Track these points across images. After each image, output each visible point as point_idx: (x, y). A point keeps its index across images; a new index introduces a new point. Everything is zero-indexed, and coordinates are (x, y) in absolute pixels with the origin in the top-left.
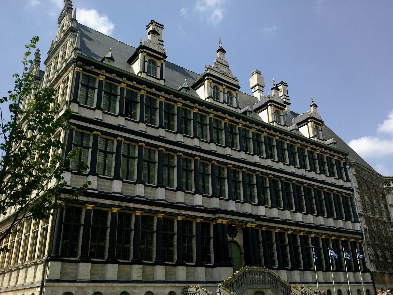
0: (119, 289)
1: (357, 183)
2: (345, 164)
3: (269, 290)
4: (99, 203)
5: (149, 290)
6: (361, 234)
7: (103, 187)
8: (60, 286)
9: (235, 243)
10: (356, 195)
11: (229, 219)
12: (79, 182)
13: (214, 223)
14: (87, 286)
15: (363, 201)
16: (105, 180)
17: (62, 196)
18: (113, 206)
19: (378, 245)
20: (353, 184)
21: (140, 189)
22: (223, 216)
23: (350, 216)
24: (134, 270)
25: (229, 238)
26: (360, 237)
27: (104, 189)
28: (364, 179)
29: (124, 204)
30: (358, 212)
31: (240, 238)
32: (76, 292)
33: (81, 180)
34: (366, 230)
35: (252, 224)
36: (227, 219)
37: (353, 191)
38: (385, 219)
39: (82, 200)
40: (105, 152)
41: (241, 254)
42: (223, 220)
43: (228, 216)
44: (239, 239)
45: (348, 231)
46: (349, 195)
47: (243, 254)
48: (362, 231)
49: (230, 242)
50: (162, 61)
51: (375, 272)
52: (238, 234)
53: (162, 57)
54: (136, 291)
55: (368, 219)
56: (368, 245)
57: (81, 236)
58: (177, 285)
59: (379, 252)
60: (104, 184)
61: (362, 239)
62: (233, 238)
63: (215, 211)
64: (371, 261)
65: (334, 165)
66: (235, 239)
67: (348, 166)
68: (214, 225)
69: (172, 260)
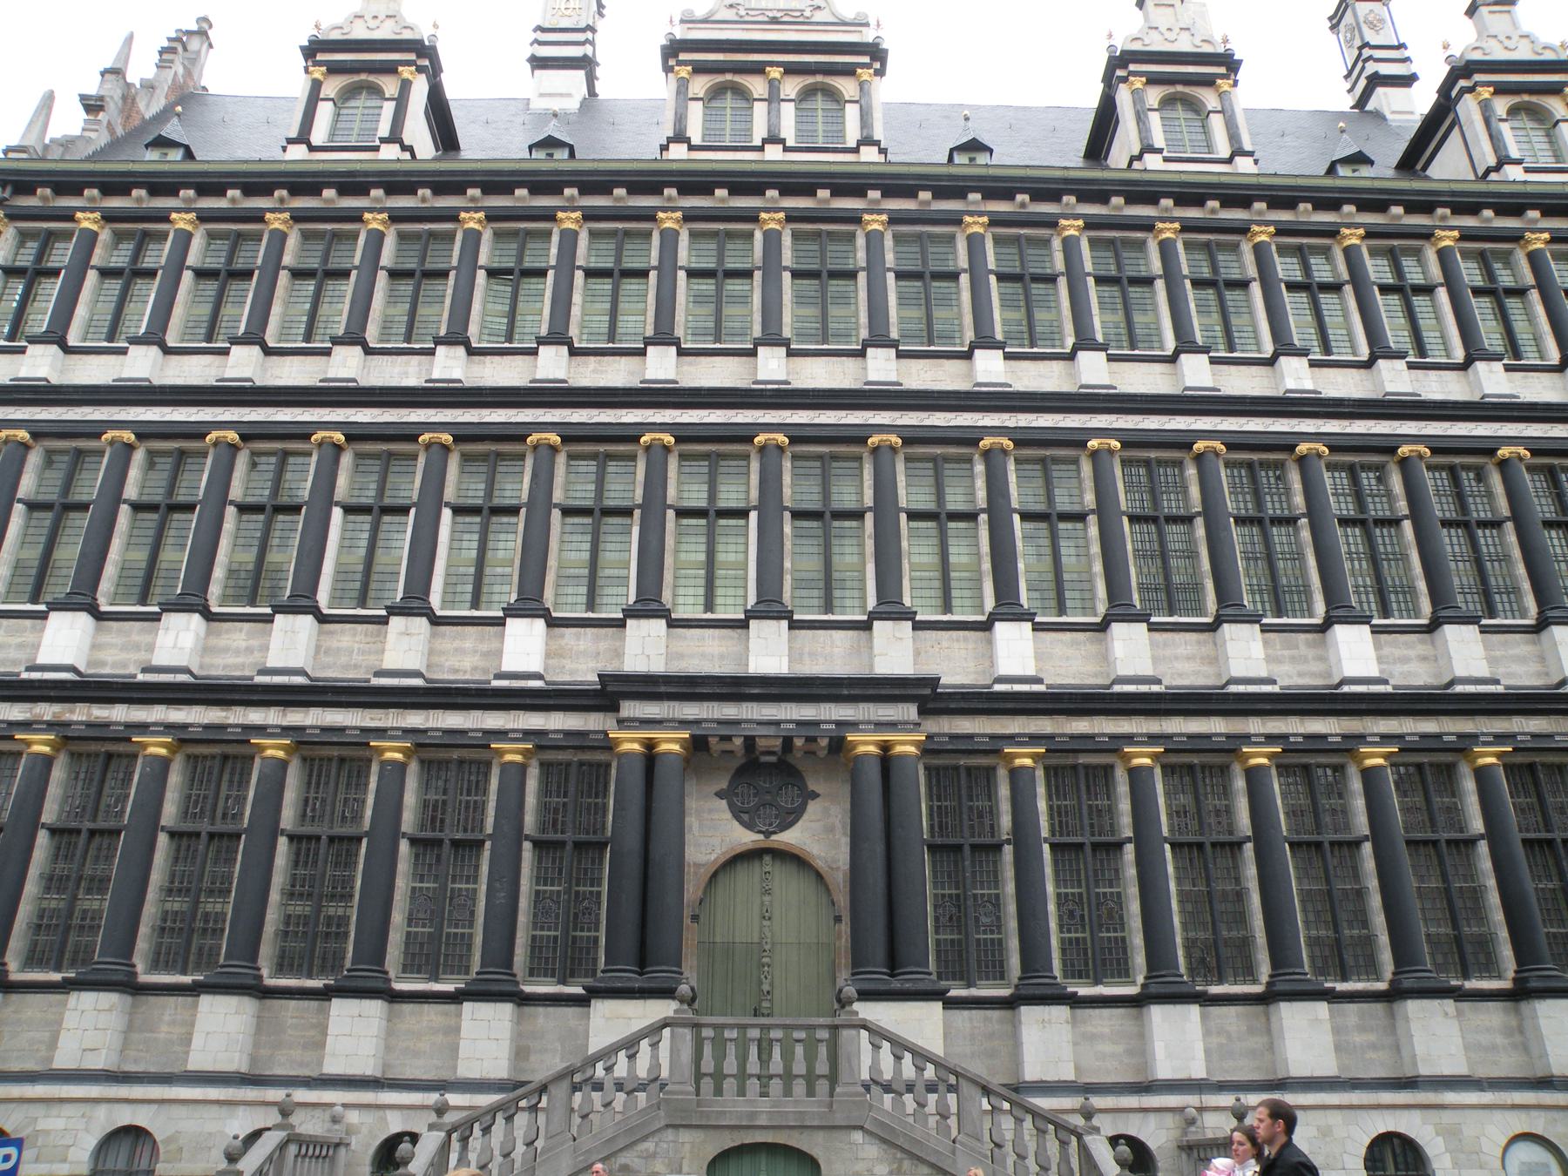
3: (858, 1136)
9: (794, 859)
16: (28, 622)
18: (26, 725)
24: (70, 1019)
29: (80, 713)
31: (830, 829)
35: (873, 731)
41: (838, 919)
47: (846, 918)
52: (813, 807)
60: (19, 640)
62: (768, 834)
63: (611, 692)
66: (790, 838)
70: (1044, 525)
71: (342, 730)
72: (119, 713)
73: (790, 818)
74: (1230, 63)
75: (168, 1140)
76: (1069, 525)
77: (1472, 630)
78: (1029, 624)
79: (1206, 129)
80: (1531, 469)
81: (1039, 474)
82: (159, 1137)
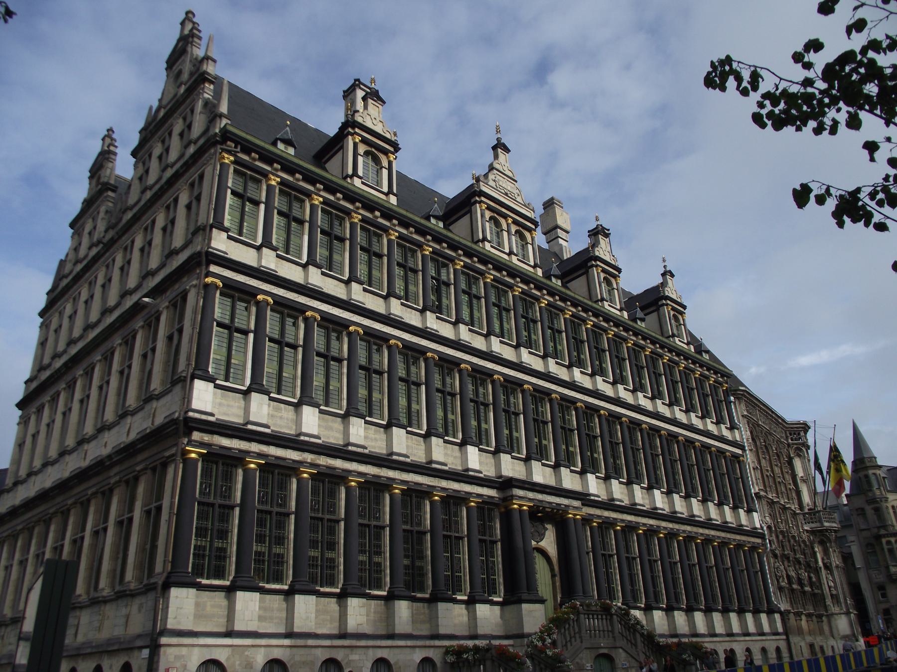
0: (318, 652)
1: (748, 433)
2: (727, 393)
3: (621, 650)
4: (272, 456)
5: (380, 654)
6: (762, 536)
7: (279, 422)
8: (193, 646)
9: (543, 552)
10: (750, 458)
11: (533, 500)
12: (228, 406)
13: (503, 510)
14: (253, 646)
15: (759, 468)
16: (282, 405)
17: (196, 436)
19: (788, 558)
20: (743, 434)
21: (355, 427)
22: (521, 493)
23: (741, 500)
25: (534, 543)
26: (759, 541)
27: (280, 426)
28: (759, 425)
30: (754, 490)
32: (228, 659)
33: (232, 403)
34: (769, 527)
35: (576, 510)
36: (530, 500)
37: (742, 448)
38: (794, 506)
39: (238, 447)
40: (280, 342)
42: (523, 500)
43: (531, 495)
44: (549, 542)
45: (739, 530)
46: (735, 456)
48: (762, 528)
49: (534, 549)
50: (392, 157)
51: (789, 612)
52: (547, 533)
53: (392, 149)
54: (355, 656)
55: (771, 503)
56: (775, 556)
57: (236, 531)
58: (437, 643)
59: (793, 574)
61: (764, 545)
62: (538, 542)
64: (781, 589)
65: (708, 396)
66: (543, 544)
67: (732, 398)
68: (501, 514)
69: (422, 589)
70: (226, 331)
71: (422, 484)
72: (338, 463)
73: (541, 536)
74: (397, 148)
75: (396, 663)
76: (239, 335)
77: (441, 440)
78: (212, 385)
79: (378, 173)
80: (531, 395)
81: (229, 304)
82: (392, 662)
